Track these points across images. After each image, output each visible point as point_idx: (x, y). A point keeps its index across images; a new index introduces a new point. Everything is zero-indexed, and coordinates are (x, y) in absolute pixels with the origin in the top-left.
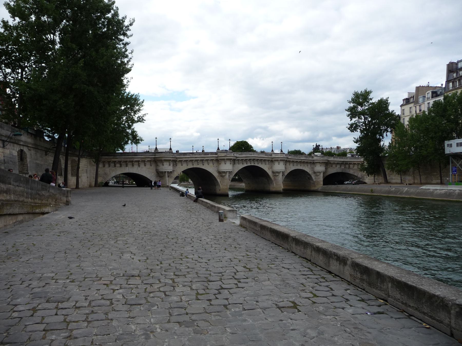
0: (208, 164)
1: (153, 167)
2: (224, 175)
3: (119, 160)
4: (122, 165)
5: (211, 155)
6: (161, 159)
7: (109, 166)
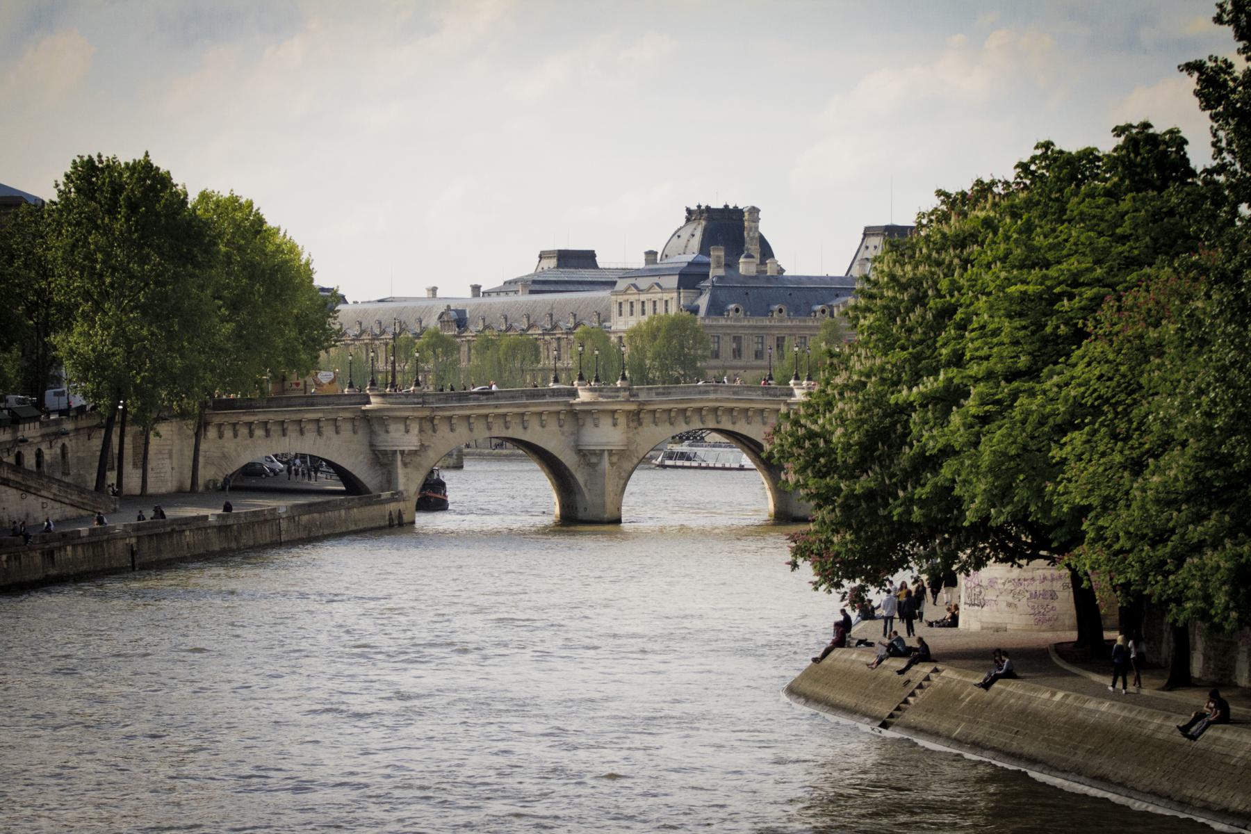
0: (543, 426)
1: (361, 436)
2: (594, 460)
3: (262, 417)
4: (271, 433)
5: (553, 396)
6: (381, 414)
7: (236, 435)
